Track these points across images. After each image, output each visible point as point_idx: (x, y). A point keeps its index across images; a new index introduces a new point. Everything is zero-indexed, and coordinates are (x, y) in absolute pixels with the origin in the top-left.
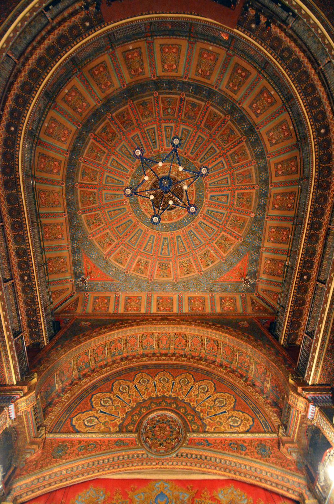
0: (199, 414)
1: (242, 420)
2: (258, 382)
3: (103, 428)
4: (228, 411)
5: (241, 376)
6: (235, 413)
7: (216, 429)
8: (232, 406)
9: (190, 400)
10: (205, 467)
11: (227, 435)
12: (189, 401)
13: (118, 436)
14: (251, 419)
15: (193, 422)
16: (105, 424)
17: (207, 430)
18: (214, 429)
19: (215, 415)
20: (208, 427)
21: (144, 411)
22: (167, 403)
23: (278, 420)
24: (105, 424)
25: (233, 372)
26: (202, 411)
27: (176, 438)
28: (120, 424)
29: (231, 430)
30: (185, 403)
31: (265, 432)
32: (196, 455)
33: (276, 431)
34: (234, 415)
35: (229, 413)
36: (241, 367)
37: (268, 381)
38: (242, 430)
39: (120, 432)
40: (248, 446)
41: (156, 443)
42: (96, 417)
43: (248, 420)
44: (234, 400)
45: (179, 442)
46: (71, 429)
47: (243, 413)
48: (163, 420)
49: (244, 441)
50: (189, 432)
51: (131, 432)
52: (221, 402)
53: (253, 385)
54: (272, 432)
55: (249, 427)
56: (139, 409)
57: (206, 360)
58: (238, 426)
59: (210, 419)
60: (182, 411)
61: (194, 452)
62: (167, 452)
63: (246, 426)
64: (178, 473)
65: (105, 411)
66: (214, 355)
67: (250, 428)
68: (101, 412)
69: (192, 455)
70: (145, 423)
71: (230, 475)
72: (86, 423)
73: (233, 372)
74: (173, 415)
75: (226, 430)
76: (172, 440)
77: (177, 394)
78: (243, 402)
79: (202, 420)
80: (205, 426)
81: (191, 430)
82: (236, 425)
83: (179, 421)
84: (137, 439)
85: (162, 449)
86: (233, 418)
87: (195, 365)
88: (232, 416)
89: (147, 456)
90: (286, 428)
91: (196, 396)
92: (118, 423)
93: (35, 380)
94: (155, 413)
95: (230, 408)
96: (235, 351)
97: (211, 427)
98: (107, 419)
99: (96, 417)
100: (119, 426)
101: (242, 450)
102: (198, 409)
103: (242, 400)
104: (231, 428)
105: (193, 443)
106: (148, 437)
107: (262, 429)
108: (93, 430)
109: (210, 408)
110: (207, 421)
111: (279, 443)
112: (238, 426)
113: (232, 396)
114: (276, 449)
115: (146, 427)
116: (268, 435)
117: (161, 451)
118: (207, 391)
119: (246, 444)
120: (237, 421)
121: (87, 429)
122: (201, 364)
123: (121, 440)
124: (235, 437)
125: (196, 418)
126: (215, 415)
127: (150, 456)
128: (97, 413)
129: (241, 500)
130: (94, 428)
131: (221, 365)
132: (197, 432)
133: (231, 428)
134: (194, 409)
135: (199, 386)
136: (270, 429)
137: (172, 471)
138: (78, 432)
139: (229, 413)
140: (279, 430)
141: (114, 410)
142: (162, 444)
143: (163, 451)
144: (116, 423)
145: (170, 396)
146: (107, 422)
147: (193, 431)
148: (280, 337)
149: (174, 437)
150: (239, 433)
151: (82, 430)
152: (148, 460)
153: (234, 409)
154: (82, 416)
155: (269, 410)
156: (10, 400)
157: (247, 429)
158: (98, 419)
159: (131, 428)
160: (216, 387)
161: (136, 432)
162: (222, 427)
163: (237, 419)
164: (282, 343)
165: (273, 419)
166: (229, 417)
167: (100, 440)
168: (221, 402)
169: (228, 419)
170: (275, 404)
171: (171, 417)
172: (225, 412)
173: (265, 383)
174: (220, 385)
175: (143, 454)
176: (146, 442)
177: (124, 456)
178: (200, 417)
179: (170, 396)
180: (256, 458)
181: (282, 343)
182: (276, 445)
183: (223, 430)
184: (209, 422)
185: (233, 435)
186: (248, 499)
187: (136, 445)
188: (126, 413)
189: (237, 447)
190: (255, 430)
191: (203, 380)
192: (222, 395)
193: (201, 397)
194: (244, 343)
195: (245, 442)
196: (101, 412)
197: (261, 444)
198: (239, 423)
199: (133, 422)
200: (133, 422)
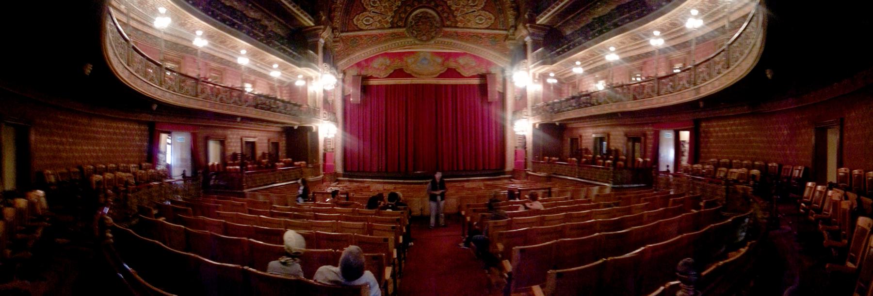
3: (378, 25)
6: (483, 13)
11: (472, 30)
13: (391, 31)
14: (493, 18)
15: (448, 19)
16: (380, 21)
21: (409, 9)
24: (380, 21)
39: (392, 27)
43: (490, 19)
48: (425, 16)
50: (444, 26)
51: (400, 27)
60: (440, 8)
61: (447, 40)
62: (428, 40)
70: (410, 19)
79: (455, 17)
80: (457, 22)
83: (438, 18)
85: (424, 38)
93: (324, 18)
100: (392, 23)
102: (453, 8)
105: (446, 35)
109: (464, 6)
110: (459, 18)
111: (506, 37)
120: (481, 20)
134: (449, 7)
138: (361, 30)
147: (448, 26)
153: (483, 9)
154: (360, 17)
156: (317, 36)
159: (400, 24)
176: (412, 33)
189: (476, 38)
199: (401, 19)
200: (401, 19)
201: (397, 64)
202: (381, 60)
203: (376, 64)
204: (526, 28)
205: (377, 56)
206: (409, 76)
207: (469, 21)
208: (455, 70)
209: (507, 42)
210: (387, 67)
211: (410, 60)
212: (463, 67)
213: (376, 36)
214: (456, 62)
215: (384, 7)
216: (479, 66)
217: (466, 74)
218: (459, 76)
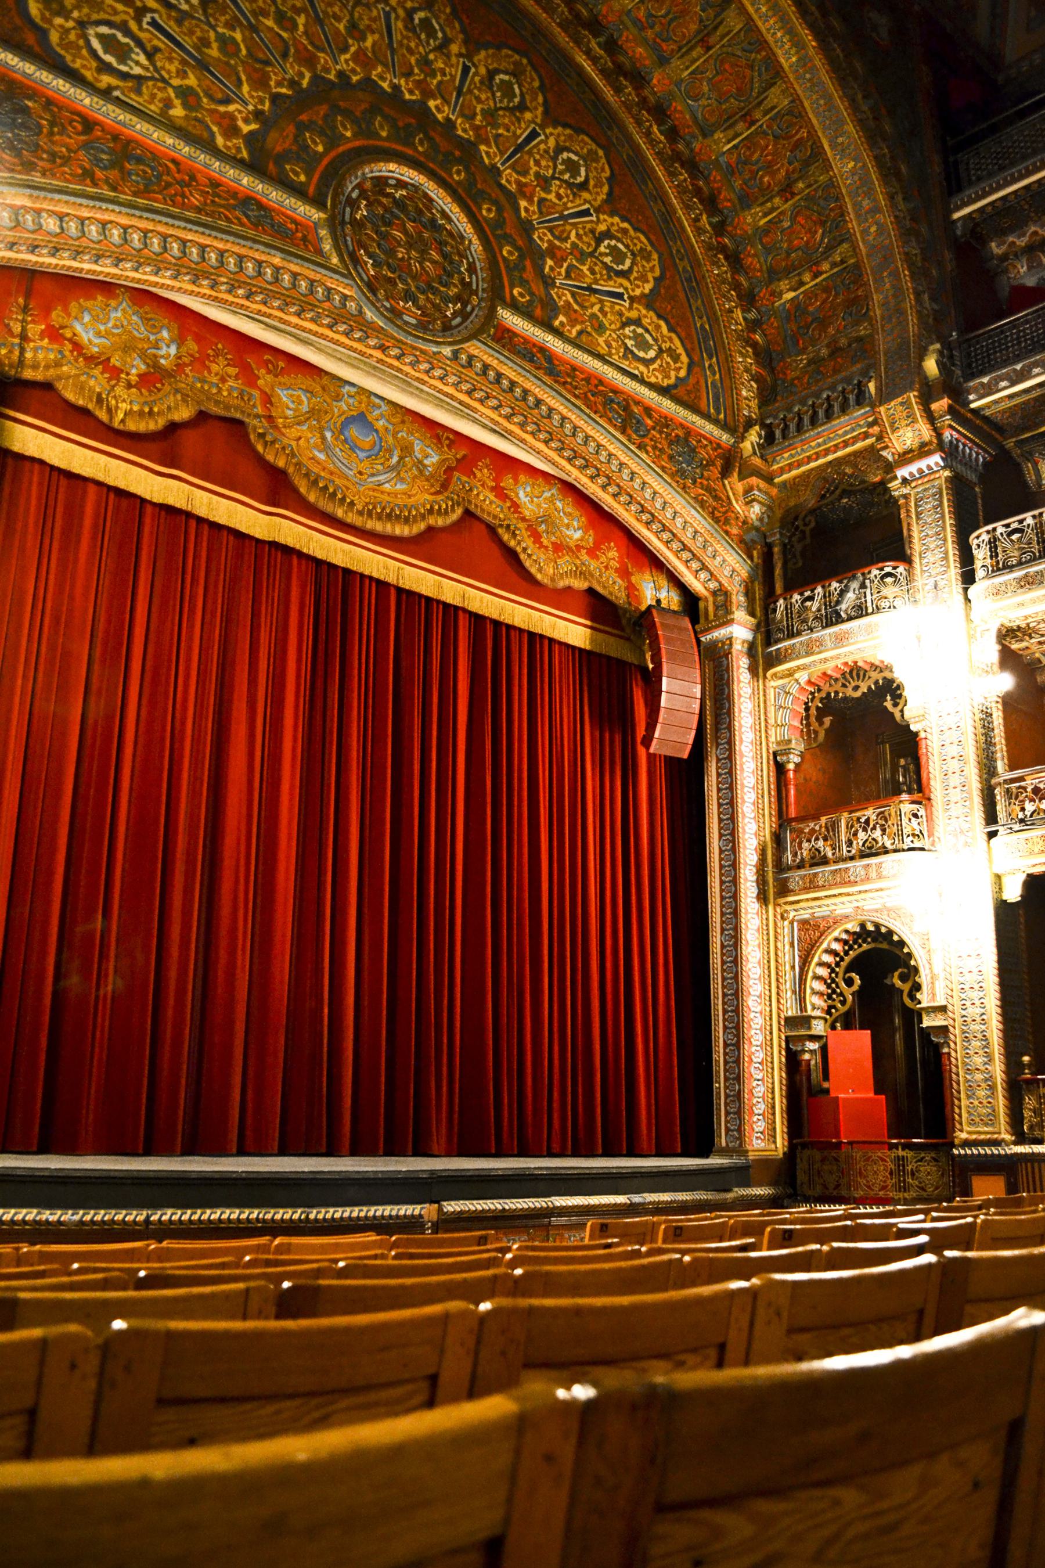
0: (542, 257)
1: (660, 350)
2: (755, 260)
3: (178, 111)
4: (632, 299)
5: (711, 203)
6: (649, 318)
7: (584, 338)
8: (648, 287)
9: (518, 183)
10: (522, 426)
12: (513, 188)
16: (186, 94)
17: (557, 323)
18: (580, 333)
19: (589, 289)
20: (562, 318)
22: (434, 147)
23: (754, 404)
24: (186, 94)
25: (692, 166)
26: (552, 251)
27: (458, 298)
28: (251, 133)
29: (625, 364)
30: (501, 186)
31: (707, 417)
32: (513, 384)
33: (737, 428)
34: (645, 321)
35: (631, 308)
36: (731, 171)
37: (802, 284)
38: (653, 380)
39: (253, 167)
40: (654, 428)
41: (391, 282)
42: (139, 43)
44: (657, 273)
45: (465, 316)
46: (31, 39)
47: (671, 329)
49: (648, 410)
52: (618, 256)
53: (735, 260)
54: (725, 426)
55: (672, 381)
56: (323, 109)
57: (612, 46)
58: (647, 362)
59: (573, 295)
63: (665, 371)
64: (419, 394)
65: (171, 27)
66: (655, 48)
67: (675, 386)
68: (154, 23)
69: (499, 376)
71: (575, 473)
72: (96, 44)
73: (692, 166)
74: (454, 210)
75: (610, 355)
76: (446, 300)
77: (476, 128)
78: (682, 295)
79: (548, 282)
81: (508, 299)
82: (641, 354)
84: (323, 233)
86: (640, 330)
87: (563, 39)
88: (637, 322)
89: (360, 312)
90: (770, 439)
91: (545, 183)
92: (246, 129)
94: (392, 166)
95: (638, 292)
96: (767, 104)
97: (573, 322)
98: (192, 81)
99: (139, 43)
101: (636, 431)
102: (542, 238)
103: (679, 287)
104: (625, 357)
106: (362, 245)
107: (703, 405)
108: (134, 99)
109: (582, 256)
111: (729, 462)
112: (647, 362)
113: (655, 256)
114: (715, 472)
115: (353, 204)
116: (709, 428)
117: (406, 318)
118: (584, 186)
119: (649, 422)
120: (647, 347)
121: (106, 80)
122: (588, 53)
123: (260, 206)
124: (627, 388)
125: (528, 263)
126: (589, 289)
127: (369, 314)
128: (139, 21)
129: (568, 526)
130: (139, 92)
131: (660, 112)
132: (526, 313)
133: (625, 357)
135: (559, 149)
136: (722, 416)
137: (405, 384)
139: (631, 308)
140: (746, 430)
141: (214, 52)
142: (408, 296)
143: (414, 321)
144: (231, 117)
145: (450, 124)
146: (190, 88)
147: (515, 307)
148: (971, 192)
149: (453, 291)
150: (642, 381)
151: (88, 75)
152: (358, 324)
153: (649, 301)
155: (743, 361)
157: (666, 383)
158: (150, 56)
160: (617, 191)
161: (318, 203)
162: (601, 340)
163: (647, 336)
164: (956, 216)
165: (744, 393)
166: (629, 322)
167: (174, 161)
168: (618, 256)
169: (624, 325)
170: (765, 357)
171: (445, 215)
172: (620, 296)
173: (784, 285)
174: (629, 192)
175: (345, 298)
177: (277, 269)
178: (543, 270)
179: (450, 124)
180: (663, 468)
181: (956, 216)
182: (719, 463)
183: (602, 352)
184: (567, 303)
185: (627, 380)
186: (585, 532)
187: (319, 252)
188: (275, 98)
189: (627, 417)
190: (686, 398)
191: (578, 131)
192: (625, 231)
193: (559, 197)
194: (850, 127)
195: (650, 417)
196: (154, 23)
197: (687, 440)
198: (652, 354)
201: (223, 386)
202: (120, 314)
203: (90, 326)
204: (931, 418)
205: (106, 288)
206: (277, 488)
207: (600, 328)
208: (492, 530)
209: (735, 485)
210: (153, 378)
211: (290, 398)
212: (536, 536)
213: (149, 157)
214: (500, 493)
215: (225, 43)
216: (592, 553)
217: (542, 566)
218: (514, 573)
